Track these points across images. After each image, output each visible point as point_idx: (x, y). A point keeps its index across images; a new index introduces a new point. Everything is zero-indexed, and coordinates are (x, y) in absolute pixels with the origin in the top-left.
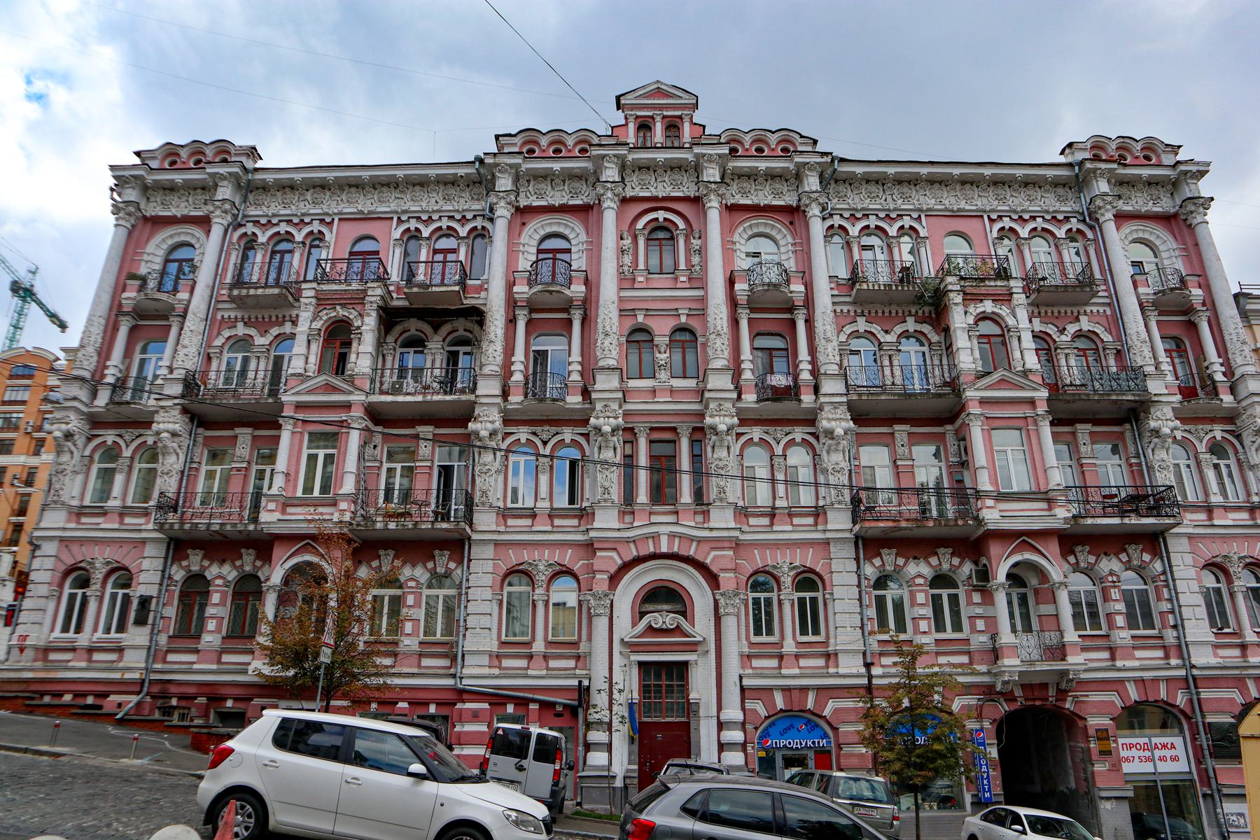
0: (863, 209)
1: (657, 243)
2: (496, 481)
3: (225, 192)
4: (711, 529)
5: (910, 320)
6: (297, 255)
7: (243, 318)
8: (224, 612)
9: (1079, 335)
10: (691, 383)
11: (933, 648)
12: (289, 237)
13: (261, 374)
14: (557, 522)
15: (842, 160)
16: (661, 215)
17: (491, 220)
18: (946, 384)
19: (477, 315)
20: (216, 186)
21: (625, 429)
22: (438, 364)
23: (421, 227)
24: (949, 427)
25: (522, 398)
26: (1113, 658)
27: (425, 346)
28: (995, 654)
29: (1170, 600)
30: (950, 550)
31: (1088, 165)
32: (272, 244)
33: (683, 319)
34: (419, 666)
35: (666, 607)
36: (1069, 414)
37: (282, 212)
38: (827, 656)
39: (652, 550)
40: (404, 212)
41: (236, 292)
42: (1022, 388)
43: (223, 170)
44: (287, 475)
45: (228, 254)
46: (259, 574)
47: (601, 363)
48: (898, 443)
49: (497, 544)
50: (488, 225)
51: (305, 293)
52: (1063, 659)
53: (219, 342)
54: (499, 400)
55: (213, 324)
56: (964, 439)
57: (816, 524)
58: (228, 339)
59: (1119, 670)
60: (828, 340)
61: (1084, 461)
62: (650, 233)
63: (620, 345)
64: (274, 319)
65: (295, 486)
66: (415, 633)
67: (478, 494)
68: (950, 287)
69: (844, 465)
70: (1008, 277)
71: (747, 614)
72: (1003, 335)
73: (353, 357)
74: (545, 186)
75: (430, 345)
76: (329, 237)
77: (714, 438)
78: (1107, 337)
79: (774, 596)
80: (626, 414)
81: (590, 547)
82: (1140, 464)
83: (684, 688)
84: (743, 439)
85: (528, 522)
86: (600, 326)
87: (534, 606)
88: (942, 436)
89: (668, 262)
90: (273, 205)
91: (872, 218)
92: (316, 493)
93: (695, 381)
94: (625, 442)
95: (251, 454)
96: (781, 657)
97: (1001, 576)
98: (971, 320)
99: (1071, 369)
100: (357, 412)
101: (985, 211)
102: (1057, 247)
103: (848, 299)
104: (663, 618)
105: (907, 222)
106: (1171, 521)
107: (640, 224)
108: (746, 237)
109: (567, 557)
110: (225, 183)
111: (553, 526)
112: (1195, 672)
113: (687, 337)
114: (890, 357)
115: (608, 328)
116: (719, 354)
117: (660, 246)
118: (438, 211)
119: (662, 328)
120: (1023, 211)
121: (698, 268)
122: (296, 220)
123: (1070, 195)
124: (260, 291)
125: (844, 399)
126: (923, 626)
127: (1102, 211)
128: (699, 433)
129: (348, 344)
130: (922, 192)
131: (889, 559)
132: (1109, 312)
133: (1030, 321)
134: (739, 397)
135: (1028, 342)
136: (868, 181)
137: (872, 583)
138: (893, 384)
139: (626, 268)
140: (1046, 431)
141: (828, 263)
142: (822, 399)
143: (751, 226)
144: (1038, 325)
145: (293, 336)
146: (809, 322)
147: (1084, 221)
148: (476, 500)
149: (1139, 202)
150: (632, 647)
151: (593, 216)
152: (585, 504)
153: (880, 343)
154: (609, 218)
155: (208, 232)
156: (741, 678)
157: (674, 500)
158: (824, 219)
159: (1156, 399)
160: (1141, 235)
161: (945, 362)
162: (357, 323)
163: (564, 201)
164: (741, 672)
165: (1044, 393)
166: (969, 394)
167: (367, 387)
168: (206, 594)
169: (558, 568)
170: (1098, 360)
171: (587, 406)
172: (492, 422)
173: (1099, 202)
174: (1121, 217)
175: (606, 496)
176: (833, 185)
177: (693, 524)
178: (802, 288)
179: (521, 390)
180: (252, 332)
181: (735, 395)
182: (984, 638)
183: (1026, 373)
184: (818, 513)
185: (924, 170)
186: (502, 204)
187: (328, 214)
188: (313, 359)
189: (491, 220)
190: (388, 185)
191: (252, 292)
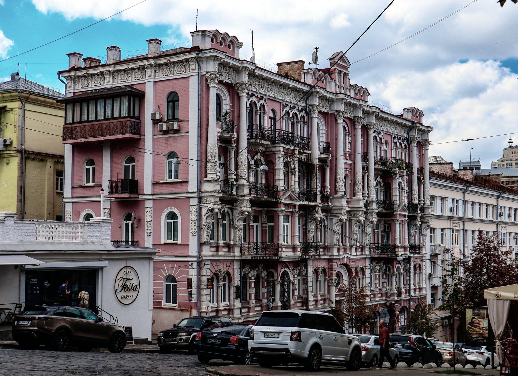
16: (344, 124)
112: (412, 298)
125: (377, 211)
147: (407, 142)
162: (293, 166)
184: (363, 248)
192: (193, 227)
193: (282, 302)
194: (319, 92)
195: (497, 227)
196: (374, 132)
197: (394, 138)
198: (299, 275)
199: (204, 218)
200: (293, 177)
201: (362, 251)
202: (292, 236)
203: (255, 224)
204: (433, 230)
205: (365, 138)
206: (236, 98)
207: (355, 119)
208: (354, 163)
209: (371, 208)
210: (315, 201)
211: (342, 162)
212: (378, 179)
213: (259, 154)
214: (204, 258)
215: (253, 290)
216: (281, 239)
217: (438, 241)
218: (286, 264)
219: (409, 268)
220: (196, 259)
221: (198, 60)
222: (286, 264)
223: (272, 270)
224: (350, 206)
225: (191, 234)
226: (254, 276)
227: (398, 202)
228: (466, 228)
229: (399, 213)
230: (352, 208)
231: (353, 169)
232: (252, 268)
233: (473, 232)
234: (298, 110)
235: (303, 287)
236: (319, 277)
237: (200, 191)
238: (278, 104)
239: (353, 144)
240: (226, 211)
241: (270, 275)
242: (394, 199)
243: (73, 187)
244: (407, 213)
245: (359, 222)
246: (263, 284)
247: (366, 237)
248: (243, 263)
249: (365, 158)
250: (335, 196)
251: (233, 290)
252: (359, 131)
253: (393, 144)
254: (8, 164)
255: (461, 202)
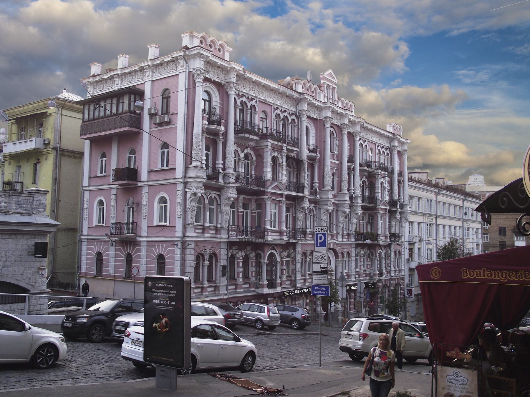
16: (332, 129)
37: (244, 91)
76: (257, 110)
147: (390, 150)
162: (281, 160)
180: (239, 150)
184: (349, 236)
192: (179, 210)
193: (268, 280)
194: (307, 99)
195: (463, 223)
196: (360, 139)
197: (378, 146)
198: (288, 256)
199: (188, 201)
200: (281, 170)
201: (348, 238)
202: (279, 222)
203: (245, 211)
204: (411, 223)
205: (352, 144)
206: (225, 96)
207: (342, 126)
208: (341, 163)
209: (356, 202)
210: (303, 192)
211: (329, 161)
212: (364, 179)
213: (249, 148)
214: (187, 239)
215: (241, 270)
216: (268, 223)
217: (416, 232)
218: (273, 246)
219: (390, 253)
220: (179, 239)
221: (186, 58)
222: (273, 247)
223: (260, 252)
224: (337, 199)
225: (177, 217)
226: (241, 256)
227: (380, 198)
228: (438, 223)
229: (381, 207)
230: (338, 201)
231: (340, 168)
232: (240, 249)
233: (444, 226)
234: (289, 113)
235: (291, 267)
236: (308, 259)
237: (185, 177)
238: (270, 108)
239: (341, 147)
240: (213, 197)
241: (258, 256)
242: (376, 195)
243: (90, 178)
244: (388, 208)
245: (345, 212)
246: (252, 264)
247: (352, 226)
248: (231, 244)
249: (351, 159)
250: (323, 189)
251: (219, 269)
252: (346, 138)
253: (377, 151)
254: (46, 159)
255: (434, 202)
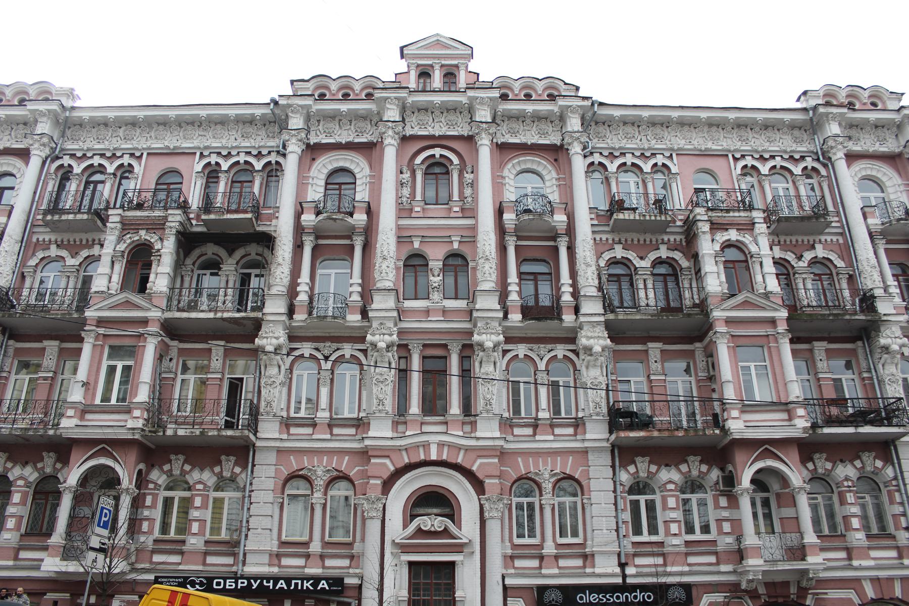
0: (620, 148)
1: (434, 176)
2: (280, 392)
3: (44, 127)
4: (478, 439)
5: (663, 248)
6: (108, 185)
7: (56, 242)
8: (25, 511)
9: (814, 262)
10: (461, 304)
11: (683, 549)
12: (102, 170)
13: (70, 291)
14: (336, 431)
15: (601, 104)
16: (437, 152)
17: (284, 155)
18: (695, 305)
19: (268, 241)
20: (36, 121)
21: (399, 346)
22: (231, 284)
23: (220, 160)
24: (698, 345)
25: (306, 316)
26: (850, 558)
27: (220, 269)
28: (740, 555)
29: (902, 504)
30: (699, 458)
31: (822, 110)
32: (86, 175)
33: (456, 245)
34: (204, 564)
35: (435, 511)
36: (805, 331)
37: (96, 147)
38: (585, 557)
39: (422, 457)
40: (206, 148)
41: (49, 217)
42: (763, 309)
43: (43, 107)
44: (85, 384)
45: (45, 183)
46: (59, 476)
47: (379, 285)
48: (652, 359)
49: (279, 451)
50: (280, 159)
51: (111, 219)
52: (803, 559)
53: (33, 262)
54: (284, 318)
55: (28, 246)
56: (711, 356)
57: (575, 434)
58: (42, 259)
59: (856, 569)
60: (588, 265)
61: (821, 376)
62: (428, 168)
63: (397, 269)
64: (84, 242)
65: (94, 395)
66: (201, 532)
67: (263, 404)
68: (698, 217)
69: (603, 380)
70: (751, 208)
71: (510, 518)
72: (746, 261)
73: (152, 277)
74: (334, 126)
75: (224, 267)
76: (137, 169)
77: (481, 354)
78: (840, 263)
79: (535, 500)
80: (401, 333)
81: (365, 455)
82: (871, 378)
83: (451, 588)
84: (509, 356)
85: (309, 430)
86: (378, 251)
87: (313, 509)
88: (692, 353)
89: (443, 194)
90: (88, 140)
91: (629, 156)
92: (113, 401)
93: (465, 302)
94: (400, 358)
95: (57, 365)
96: (541, 558)
97: (746, 480)
98: (717, 247)
99: (808, 293)
100: (154, 328)
101: (730, 151)
102: (794, 183)
103: (606, 229)
104: (432, 521)
105: (660, 160)
106: (901, 430)
107: (419, 160)
108: (515, 172)
109: (344, 464)
110: (45, 119)
111: (331, 434)
113: (459, 261)
114: (645, 280)
115: (385, 253)
116: (486, 274)
117: (437, 179)
118: (236, 147)
119: (436, 256)
120: (764, 151)
121: (470, 199)
122: (108, 154)
123: (805, 137)
124: (71, 217)
125: (602, 319)
126: (674, 528)
127: (834, 151)
128: (468, 350)
129: (148, 265)
130: (673, 133)
131: (643, 467)
132: (841, 241)
133: (771, 249)
134: (506, 316)
135: (769, 267)
136: (625, 123)
137: (627, 489)
138: (647, 305)
139: (404, 199)
140: (786, 348)
141: (587, 196)
142: (582, 319)
143: (519, 163)
144: (778, 253)
145: (98, 259)
146: (571, 249)
147: (818, 160)
148: (262, 410)
149: (867, 143)
150: (405, 548)
151: (375, 153)
152: (362, 414)
153: (636, 268)
154: (390, 154)
155: (27, 164)
156: (503, 578)
157: (444, 411)
158: (585, 157)
159: (885, 318)
160: (869, 172)
161: (694, 285)
162: (157, 246)
163: (350, 139)
164: (504, 571)
165: (784, 314)
166: (716, 314)
167: (164, 304)
168: (8, 494)
169: (335, 473)
170: (832, 284)
171: (366, 324)
172: (277, 338)
173: (831, 143)
174: (851, 157)
175: (381, 407)
176: (593, 126)
177: (461, 433)
178: (564, 218)
179: (305, 310)
180: (64, 253)
181: (501, 315)
182: (729, 540)
183: (767, 295)
184: (578, 424)
185: (675, 114)
186: (294, 140)
187: (137, 149)
188: (116, 278)
189: (284, 155)
190: (193, 123)
191: (64, 217)
226: (21, 478)
